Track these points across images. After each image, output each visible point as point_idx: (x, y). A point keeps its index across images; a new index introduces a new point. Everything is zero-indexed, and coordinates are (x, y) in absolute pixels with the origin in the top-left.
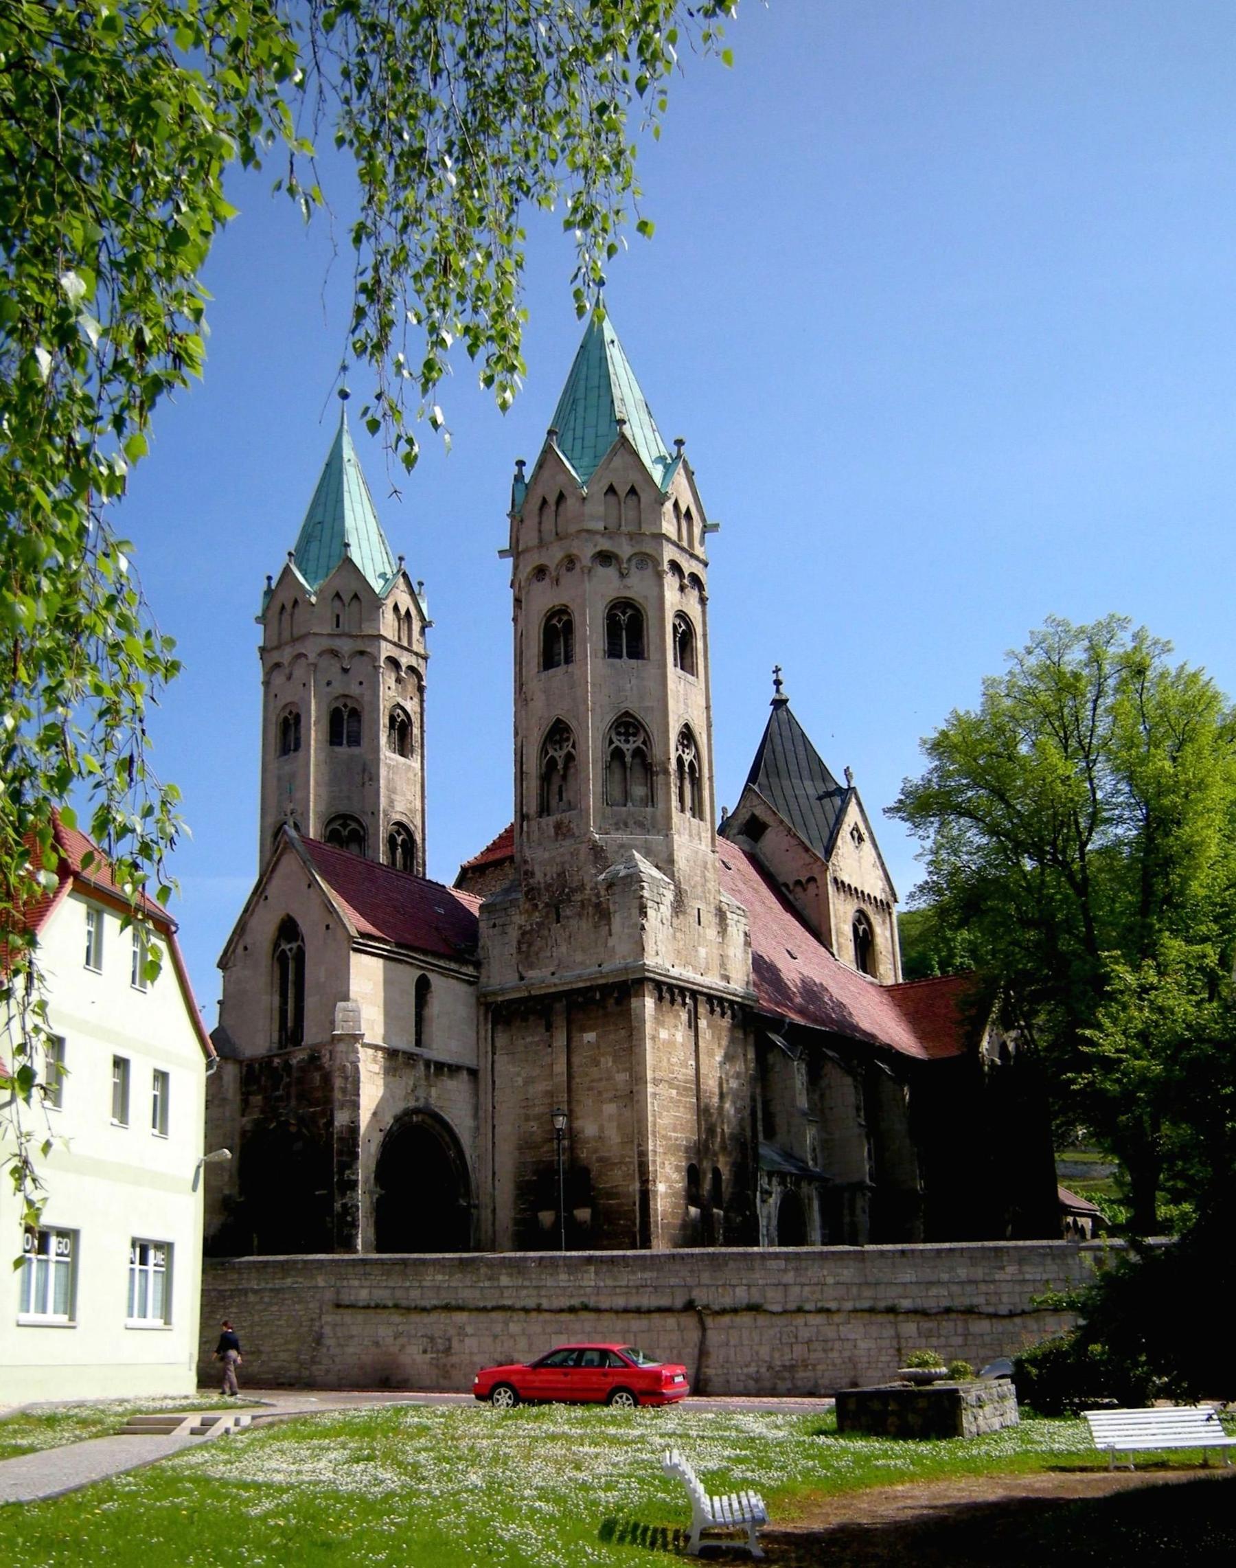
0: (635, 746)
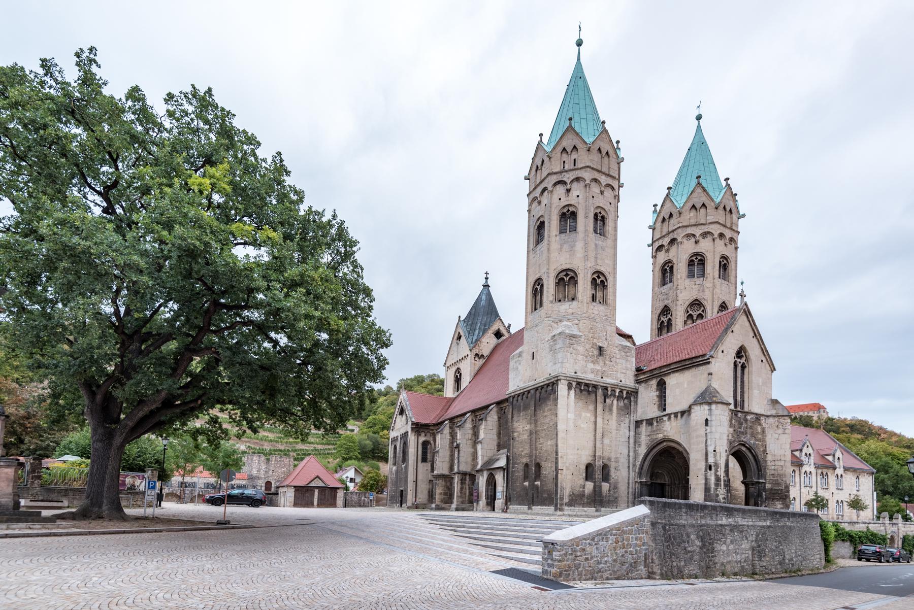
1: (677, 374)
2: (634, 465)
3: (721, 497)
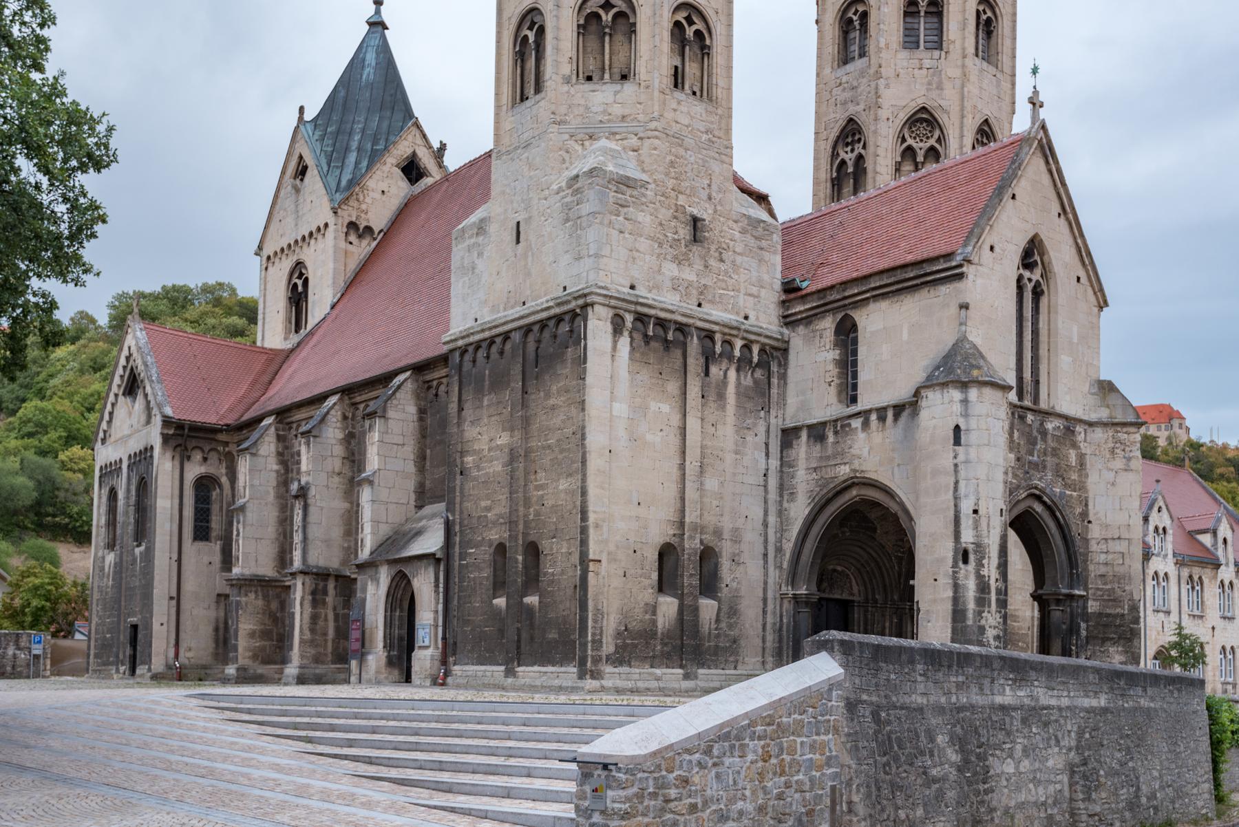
0: (928, 145)
1: (884, 305)
2: (779, 550)
3: (990, 633)
